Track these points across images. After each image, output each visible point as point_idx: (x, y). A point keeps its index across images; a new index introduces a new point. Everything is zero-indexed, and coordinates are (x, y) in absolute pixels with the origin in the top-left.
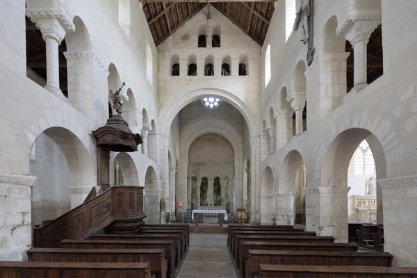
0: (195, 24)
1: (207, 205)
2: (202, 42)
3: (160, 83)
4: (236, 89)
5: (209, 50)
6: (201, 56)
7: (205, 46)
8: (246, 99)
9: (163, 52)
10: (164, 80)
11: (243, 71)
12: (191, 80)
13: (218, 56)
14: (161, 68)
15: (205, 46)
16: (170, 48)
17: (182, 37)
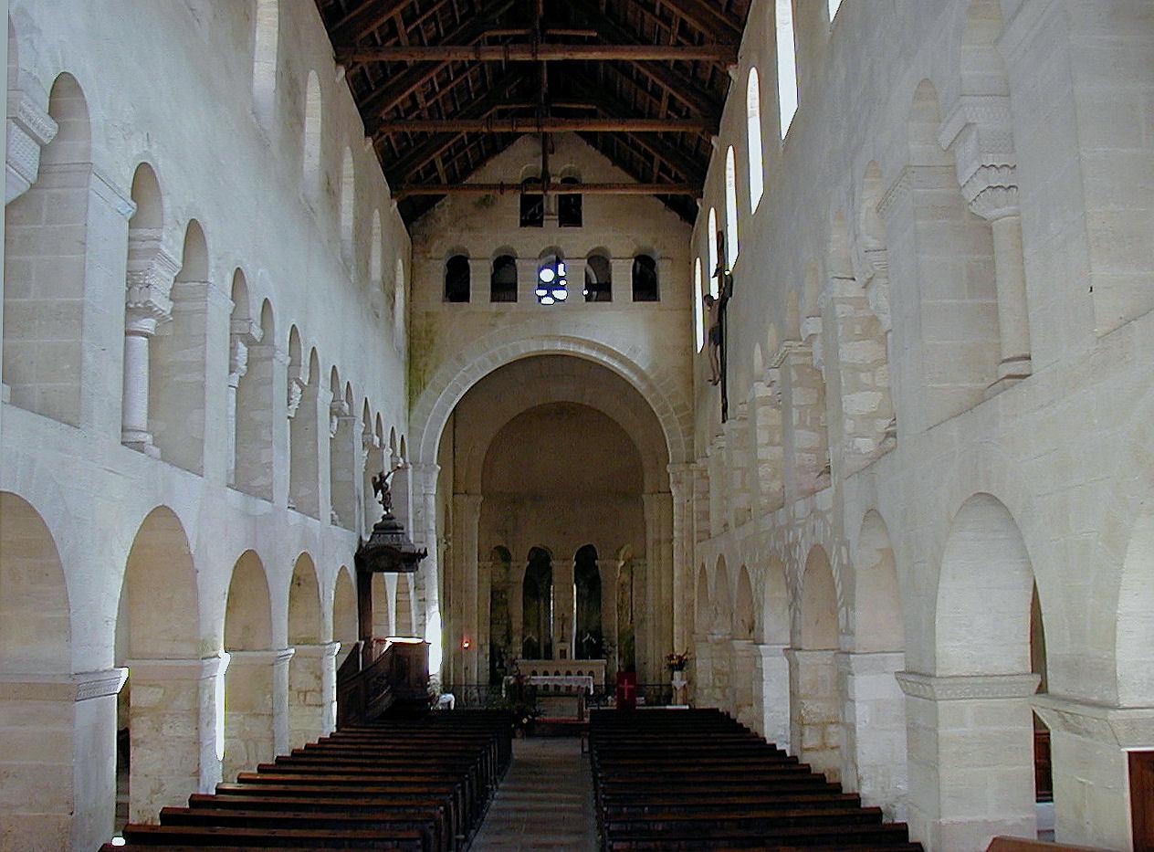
0: (516, 163)
1: (549, 655)
2: (531, 216)
3: (416, 322)
4: (622, 336)
5: (552, 233)
6: (527, 243)
7: (539, 223)
8: (654, 367)
9: (426, 239)
10: (427, 314)
11: (645, 287)
12: (499, 314)
13: (578, 242)
14: (418, 284)
15: (539, 223)
16: (445, 229)
17: (477, 200)
